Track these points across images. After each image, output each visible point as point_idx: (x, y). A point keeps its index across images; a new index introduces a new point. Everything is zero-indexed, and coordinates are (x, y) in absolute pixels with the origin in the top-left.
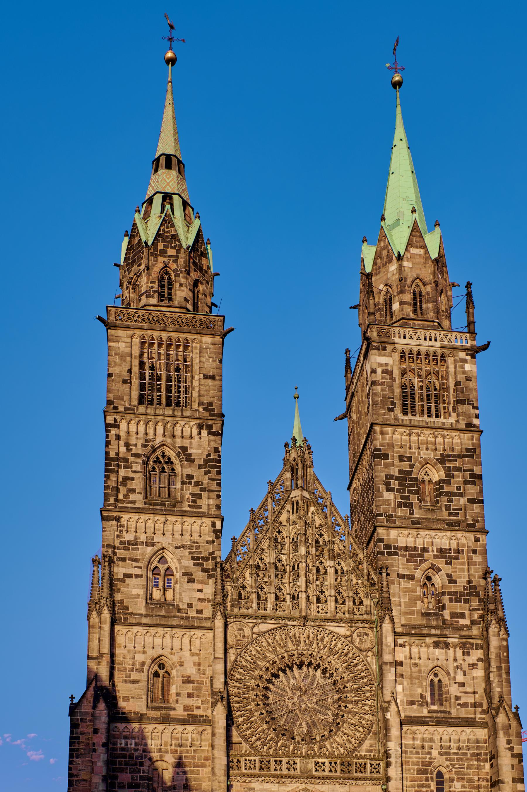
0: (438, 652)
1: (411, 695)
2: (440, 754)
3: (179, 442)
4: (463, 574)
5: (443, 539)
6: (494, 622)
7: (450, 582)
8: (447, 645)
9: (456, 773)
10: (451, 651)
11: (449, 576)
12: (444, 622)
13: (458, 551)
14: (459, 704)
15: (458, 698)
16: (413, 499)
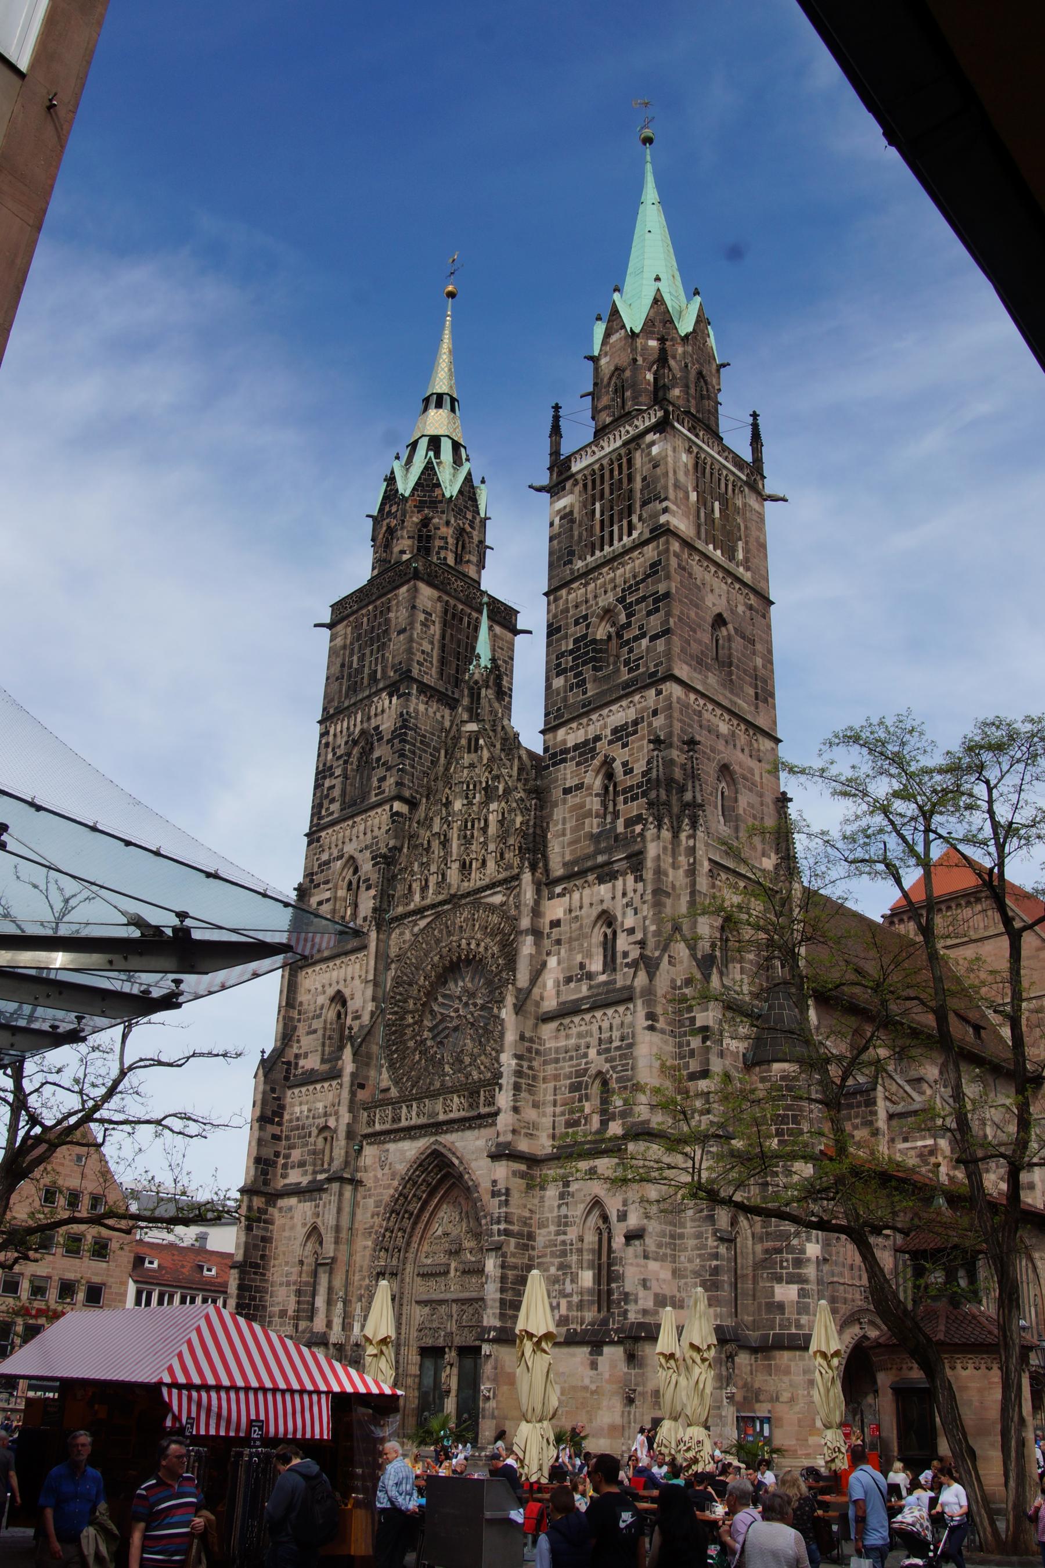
0: (603, 890)
1: (569, 968)
2: (599, 1053)
3: (374, 723)
4: (636, 757)
5: (619, 715)
6: (651, 819)
7: (625, 773)
8: (613, 876)
9: (619, 1080)
10: (619, 883)
11: (625, 764)
12: (617, 838)
13: (635, 723)
14: (627, 965)
15: (625, 954)
16: (588, 672)
